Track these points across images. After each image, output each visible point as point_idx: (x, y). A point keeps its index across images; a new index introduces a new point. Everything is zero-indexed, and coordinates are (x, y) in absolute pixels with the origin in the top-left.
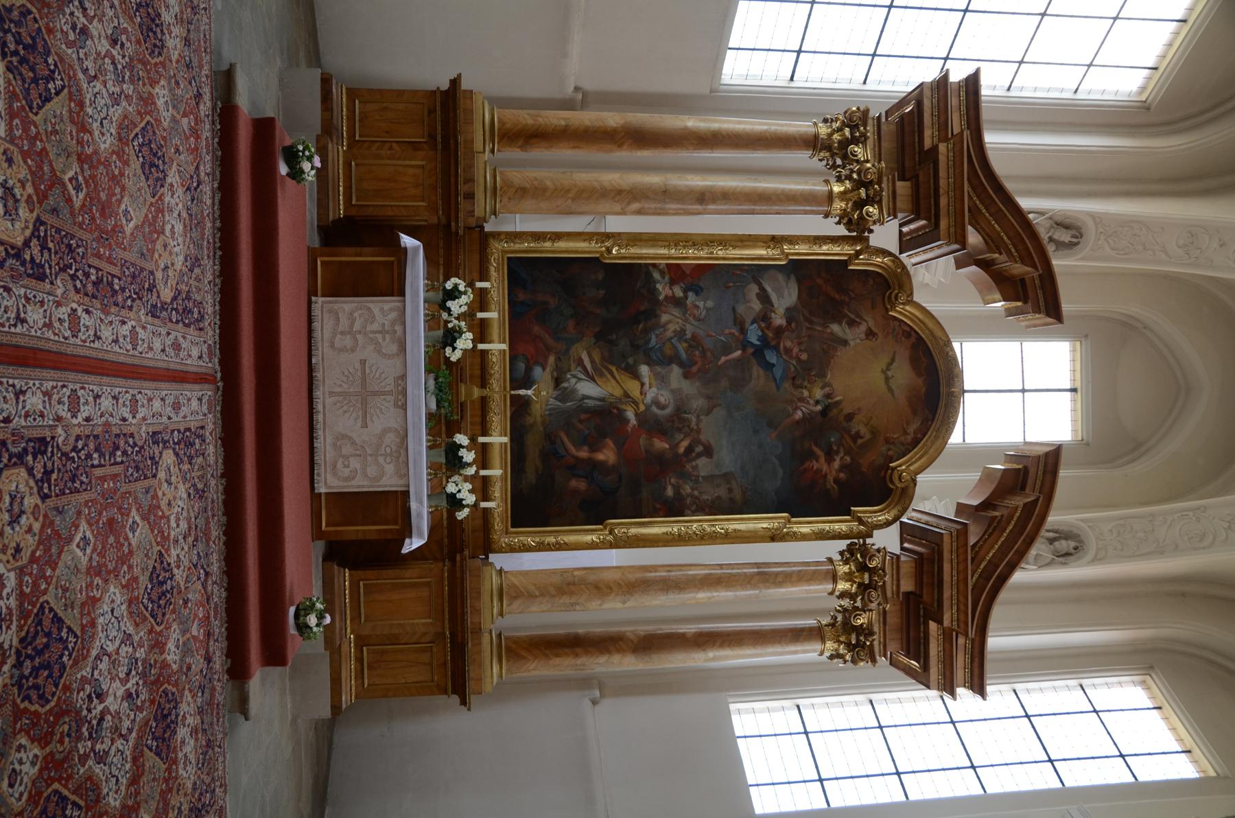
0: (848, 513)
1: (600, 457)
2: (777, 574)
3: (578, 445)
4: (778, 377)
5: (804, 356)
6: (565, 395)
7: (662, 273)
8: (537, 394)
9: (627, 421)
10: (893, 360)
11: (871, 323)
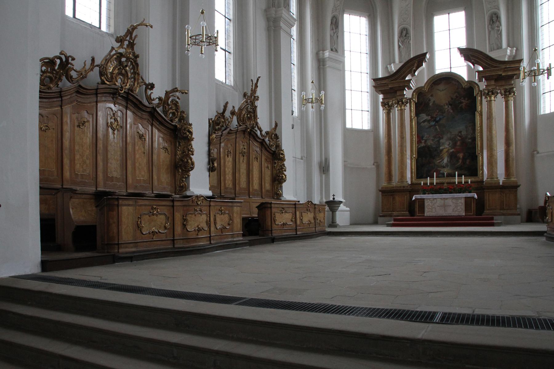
0: (476, 97)
1: (461, 157)
2: (489, 115)
4: (442, 117)
5: (438, 111)
6: (447, 165)
7: (420, 145)
8: (446, 172)
9: (453, 151)
10: (438, 89)
11: (429, 95)
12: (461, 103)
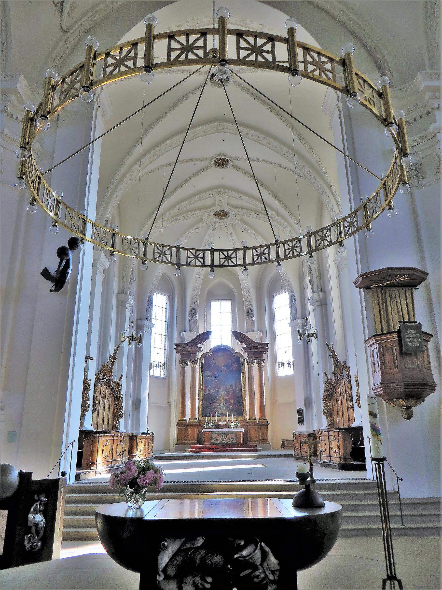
3: (230, 406)
12: (232, 366)
